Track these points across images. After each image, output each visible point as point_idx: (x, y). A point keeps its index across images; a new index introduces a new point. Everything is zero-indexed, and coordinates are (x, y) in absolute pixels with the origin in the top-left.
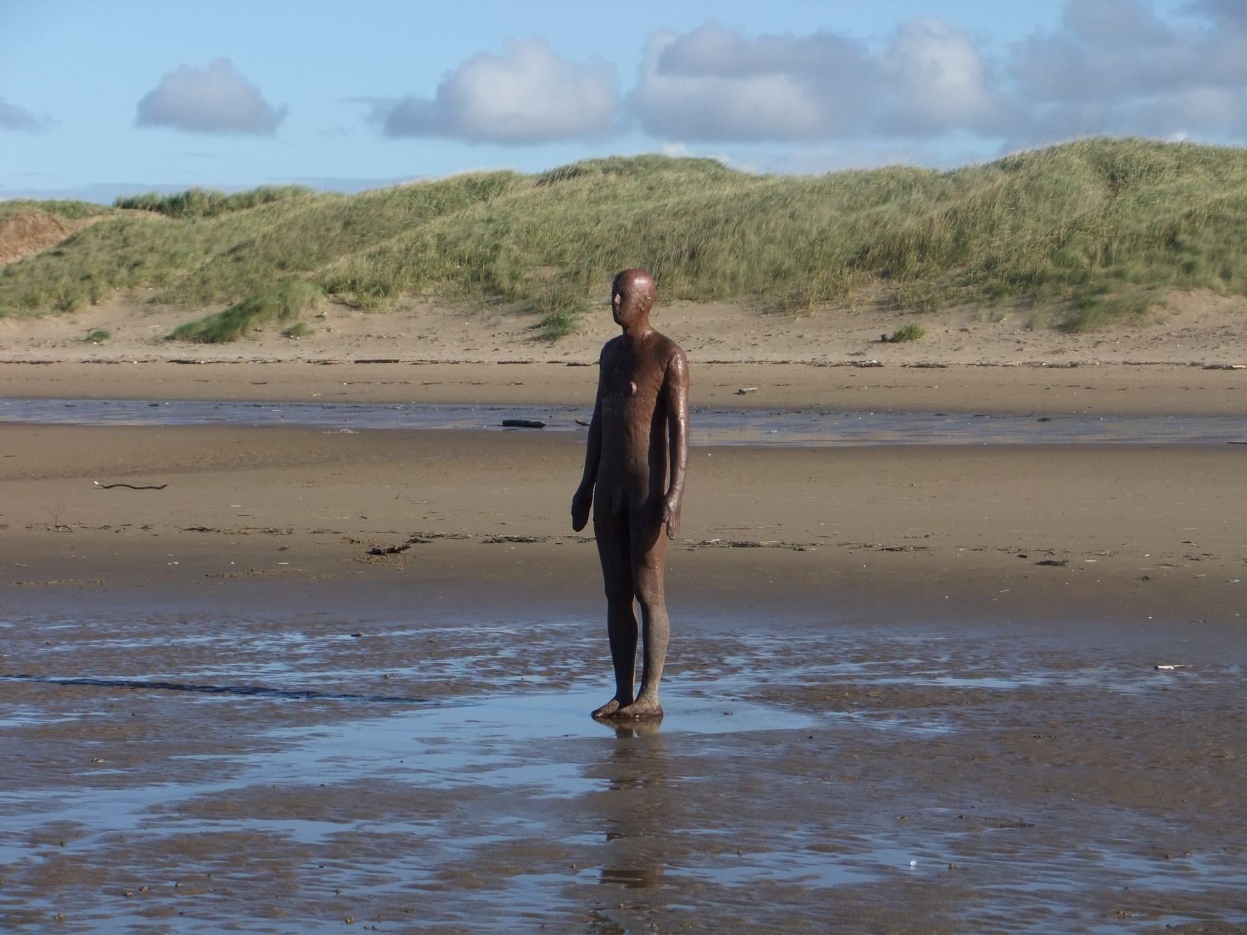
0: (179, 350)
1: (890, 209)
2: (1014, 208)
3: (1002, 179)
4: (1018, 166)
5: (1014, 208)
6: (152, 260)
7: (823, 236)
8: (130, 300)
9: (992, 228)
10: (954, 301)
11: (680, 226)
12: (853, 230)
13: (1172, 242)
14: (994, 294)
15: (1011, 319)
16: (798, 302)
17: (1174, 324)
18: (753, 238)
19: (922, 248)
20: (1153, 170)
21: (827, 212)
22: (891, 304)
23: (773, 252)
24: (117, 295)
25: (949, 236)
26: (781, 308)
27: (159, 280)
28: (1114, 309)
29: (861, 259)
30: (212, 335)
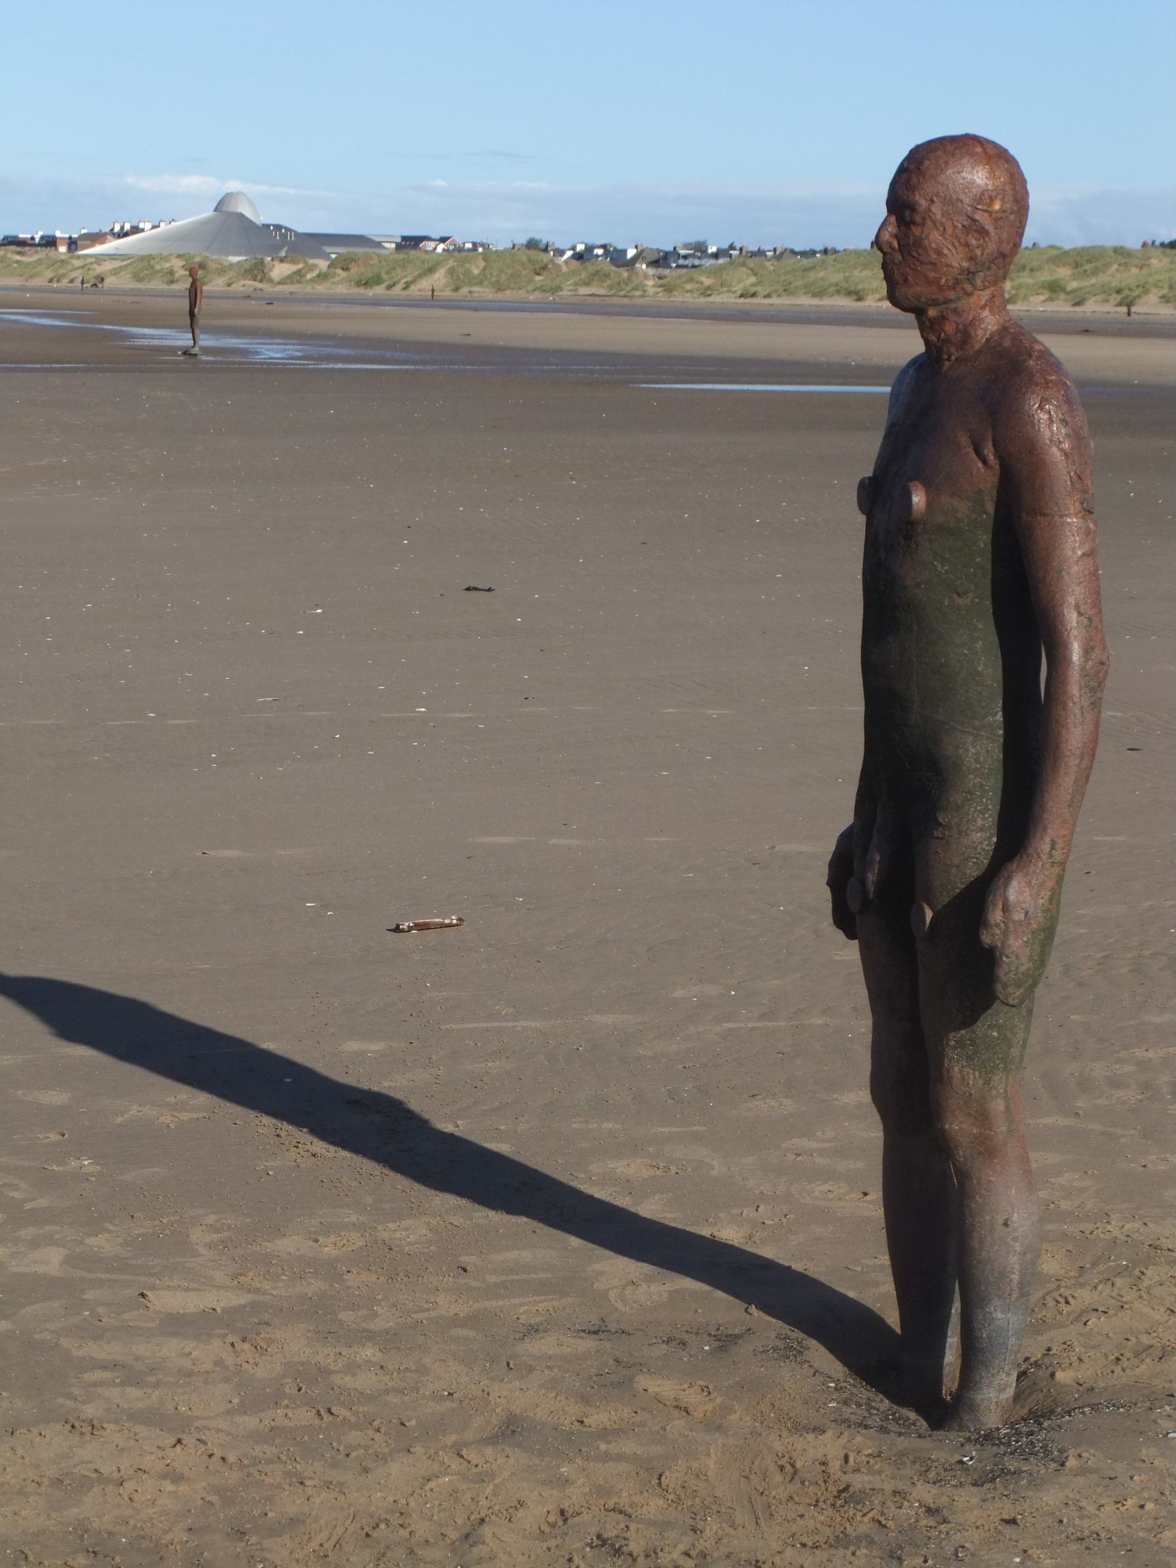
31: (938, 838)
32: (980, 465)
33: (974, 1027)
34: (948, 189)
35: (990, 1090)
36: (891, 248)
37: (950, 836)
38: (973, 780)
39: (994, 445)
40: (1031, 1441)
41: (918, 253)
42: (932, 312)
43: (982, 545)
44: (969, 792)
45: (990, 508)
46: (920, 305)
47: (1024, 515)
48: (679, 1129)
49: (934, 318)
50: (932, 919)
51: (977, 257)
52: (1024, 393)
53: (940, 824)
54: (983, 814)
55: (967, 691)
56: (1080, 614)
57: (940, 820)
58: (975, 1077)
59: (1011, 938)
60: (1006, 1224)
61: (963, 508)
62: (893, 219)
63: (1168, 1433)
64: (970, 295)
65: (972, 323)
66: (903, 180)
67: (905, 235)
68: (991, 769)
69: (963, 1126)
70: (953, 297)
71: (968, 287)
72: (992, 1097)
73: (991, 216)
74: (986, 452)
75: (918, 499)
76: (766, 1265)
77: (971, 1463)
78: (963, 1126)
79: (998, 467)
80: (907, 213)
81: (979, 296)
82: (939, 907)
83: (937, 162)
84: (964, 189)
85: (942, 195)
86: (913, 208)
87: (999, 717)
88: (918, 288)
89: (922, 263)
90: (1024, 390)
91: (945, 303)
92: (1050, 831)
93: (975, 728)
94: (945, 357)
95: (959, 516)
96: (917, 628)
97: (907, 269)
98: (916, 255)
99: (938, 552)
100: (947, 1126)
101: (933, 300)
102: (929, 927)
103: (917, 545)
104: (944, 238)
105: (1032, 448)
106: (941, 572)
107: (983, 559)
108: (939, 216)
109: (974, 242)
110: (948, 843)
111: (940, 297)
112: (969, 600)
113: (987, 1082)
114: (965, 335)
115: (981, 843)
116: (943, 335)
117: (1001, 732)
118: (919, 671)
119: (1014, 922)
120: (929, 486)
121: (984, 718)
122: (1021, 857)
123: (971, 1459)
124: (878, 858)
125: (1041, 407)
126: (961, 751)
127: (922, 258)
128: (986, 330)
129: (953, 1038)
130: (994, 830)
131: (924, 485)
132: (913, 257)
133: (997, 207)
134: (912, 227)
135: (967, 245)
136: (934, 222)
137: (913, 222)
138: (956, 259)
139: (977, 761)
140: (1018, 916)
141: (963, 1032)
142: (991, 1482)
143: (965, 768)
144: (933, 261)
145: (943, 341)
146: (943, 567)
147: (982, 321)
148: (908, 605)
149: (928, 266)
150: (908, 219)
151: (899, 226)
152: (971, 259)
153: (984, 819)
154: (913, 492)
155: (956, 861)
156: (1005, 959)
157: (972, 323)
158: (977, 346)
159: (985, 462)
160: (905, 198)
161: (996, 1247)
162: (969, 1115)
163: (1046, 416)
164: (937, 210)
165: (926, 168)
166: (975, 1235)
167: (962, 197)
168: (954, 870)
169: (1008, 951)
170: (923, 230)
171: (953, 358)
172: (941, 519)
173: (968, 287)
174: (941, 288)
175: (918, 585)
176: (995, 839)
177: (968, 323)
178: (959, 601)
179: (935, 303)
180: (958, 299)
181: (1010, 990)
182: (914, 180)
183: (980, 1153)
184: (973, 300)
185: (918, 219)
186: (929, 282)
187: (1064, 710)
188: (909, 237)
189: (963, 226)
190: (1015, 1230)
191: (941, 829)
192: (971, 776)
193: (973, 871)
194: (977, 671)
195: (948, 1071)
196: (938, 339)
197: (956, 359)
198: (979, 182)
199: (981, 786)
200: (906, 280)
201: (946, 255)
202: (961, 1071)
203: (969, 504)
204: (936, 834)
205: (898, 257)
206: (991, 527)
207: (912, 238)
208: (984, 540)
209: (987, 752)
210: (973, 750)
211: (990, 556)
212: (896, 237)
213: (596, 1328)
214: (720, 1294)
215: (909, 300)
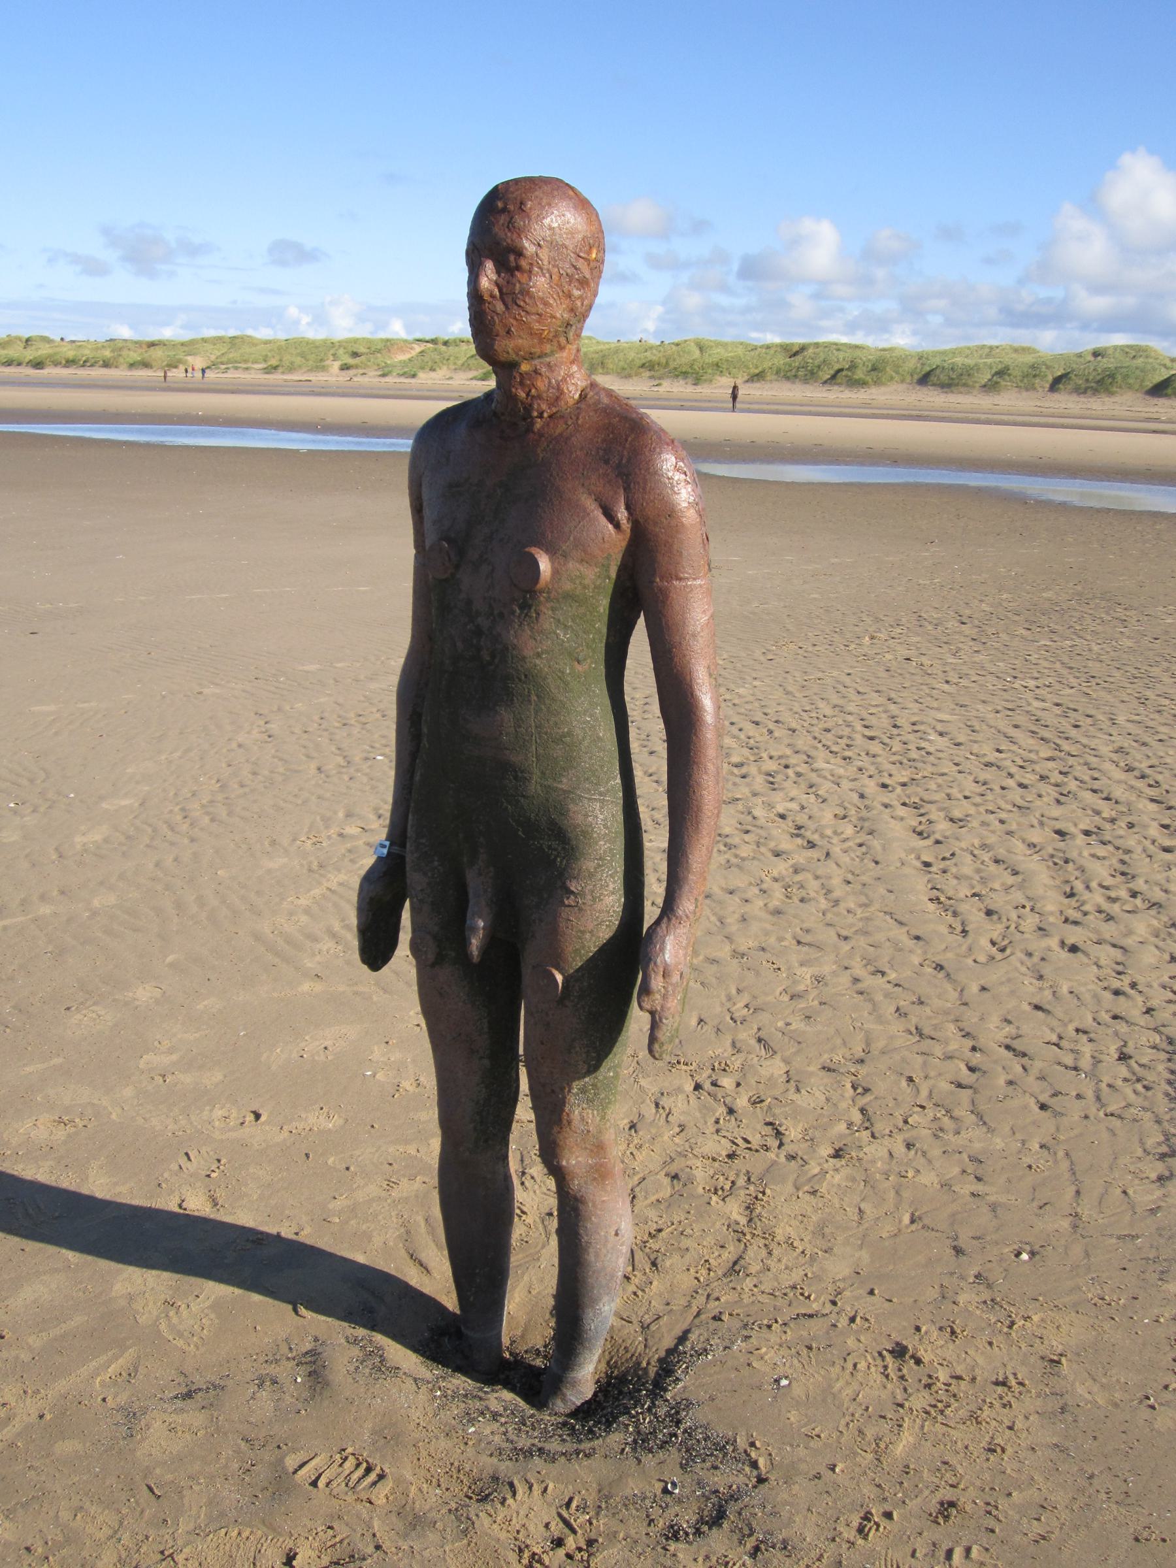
0: (475, 382)
1: (648, 354)
2: (680, 356)
3: (674, 348)
4: (677, 345)
5: (680, 356)
6: (452, 358)
7: (633, 360)
8: (449, 369)
9: (674, 360)
10: (668, 377)
11: (597, 356)
12: (640, 359)
13: (717, 365)
14: (677, 376)
15: (682, 382)
16: (629, 376)
17: (719, 384)
18: (616, 360)
19: (658, 364)
20: (712, 347)
21: (632, 355)
22: (651, 377)
23: (621, 364)
24: (445, 368)
25: (664, 361)
26: (626, 377)
27: (455, 364)
28: (706, 380)
29: (643, 366)
30: (483, 379)
31: (569, 906)
32: (610, 527)
33: (597, 1074)
34: (554, 234)
35: (605, 1124)
36: (493, 296)
37: (584, 903)
38: (603, 846)
39: (628, 508)
40: (685, 1431)
41: (525, 302)
42: (525, 367)
43: (602, 611)
44: (600, 859)
45: (613, 575)
46: (517, 359)
47: (658, 580)
48: (40, 1066)
49: (527, 373)
50: (563, 984)
51: (577, 308)
52: (660, 454)
53: (572, 892)
54: (613, 878)
55: (590, 758)
56: (710, 675)
57: (573, 889)
58: (593, 1116)
59: (670, 1000)
60: (617, 1234)
61: (590, 574)
62: (489, 266)
63: (777, 1381)
64: (562, 348)
65: (564, 380)
66: (501, 222)
67: (508, 282)
68: (616, 833)
69: (580, 1159)
70: (548, 351)
71: (563, 340)
72: (606, 1129)
73: (589, 265)
74: (619, 515)
75: (545, 564)
76: (256, 1239)
77: (677, 1491)
78: (580, 1159)
79: (629, 531)
80: (512, 258)
81: (570, 349)
82: (571, 971)
83: (540, 204)
84: (567, 234)
85: (549, 239)
86: (519, 253)
87: (618, 781)
88: (520, 341)
89: (527, 312)
90: (658, 450)
91: (539, 357)
92: (695, 891)
93: (601, 794)
94: (535, 414)
95: (586, 582)
96: (535, 698)
97: (512, 320)
98: (522, 304)
99: (562, 620)
100: (564, 1163)
101: (531, 353)
102: (562, 991)
103: (538, 614)
104: (551, 287)
105: (671, 512)
106: (563, 641)
107: (602, 626)
108: (546, 263)
109: (576, 293)
110: (580, 910)
111: (537, 350)
112: (587, 666)
113: (603, 1118)
114: (560, 393)
115: (613, 906)
116: (533, 391)
117: (621, 794)
118: (538, 741)
119: (672, 984)
120: (551, 551)
121: (607, 783)
122: (669, 920)
123: (674, 1485)
124: (481, 924)
125: (678, 470)
126: (590, 819)
127: (528, 308)
128: (575, 385)
129: (576, 1086)
130: (622, 892)
131: (547, 551)
132: (519, 306)
133: (594, 256)
134: (518, 274)
135: (569, 296)
136: (540, 268)
137: (518, 268)
138: (560, 311)
139: (606, 826)
140: (675, 978)
141: (587, 1079)
142: (722, 1518)
143: (595, 835)
144: (540, 311)
145: (533, 397)
146: (565, 635)
147: (571, 376)
148: (526, 676)
149: (533, 317)
150: (513, 264)
151: (498, 273)
152: (572, 310)
153: (615, 882)
154: (539, 559)
155: (590, 926)
156: (664, 1021)
157: (564, 380)
158: (571, 402)
159: (617, 526)
160: (509, 241)
161: (609, 1256)
162: (586, 1148)
163: (683, 476)
164: (544, 255)
165: (530, 209)
166: (591, 1250)
167: (567, 243)
168: (588, 936)
169: (666, 1014)
170: (530, 279)
171: (545, 415)
172: (568, 586)
173: (563, 340)
174: (542, 340)
175: (539, 655)
176: (623, 900)
177: (560, 378)
178: (579, 668)
179: (531, 357)
180: (553, 353)
181: (665, 1048)
182: (519, 222)
183: (595, 1179)
184: (565, 354)
185: (524, 263)
186: (532, 334)
187: (706, 773)
188: (515, 285)
189: (567, 275)
190: (623, 1236)
191: (572, 897)
192: (602, 843)
193: (605, 933)
194: (599, 738)
195: (568, 1114)
196: (528, 395)
197: (550, 417)
198: (580, 227)
199: (611, 850)
200: (509, 332)
201: (551, 305)
202: (580, 1114)
203: (597, 570)
204: (566, 902)
205: (500, 307)
206: (610, 591)
207: (518, 285)
208: (603, 605)
209: (613, 815)
210: (601, 817)
211: (605, 619)
212: (497, 284)
213: (185, 1390)
214: (256, 1298)
215: (508, 353)
